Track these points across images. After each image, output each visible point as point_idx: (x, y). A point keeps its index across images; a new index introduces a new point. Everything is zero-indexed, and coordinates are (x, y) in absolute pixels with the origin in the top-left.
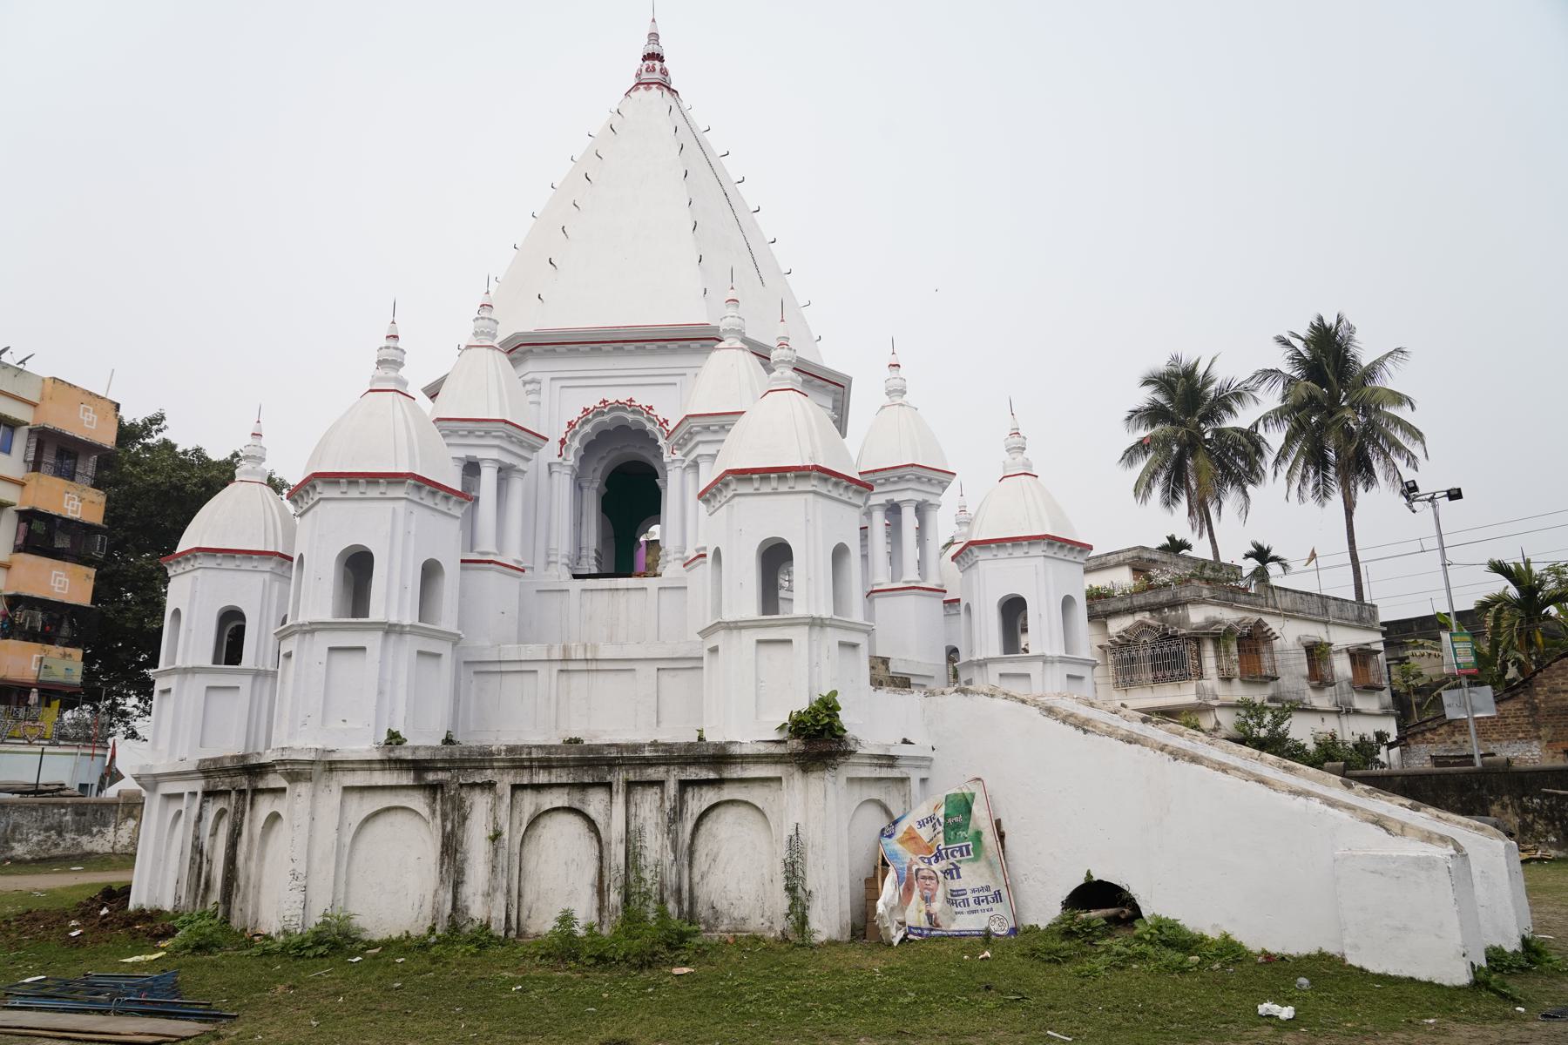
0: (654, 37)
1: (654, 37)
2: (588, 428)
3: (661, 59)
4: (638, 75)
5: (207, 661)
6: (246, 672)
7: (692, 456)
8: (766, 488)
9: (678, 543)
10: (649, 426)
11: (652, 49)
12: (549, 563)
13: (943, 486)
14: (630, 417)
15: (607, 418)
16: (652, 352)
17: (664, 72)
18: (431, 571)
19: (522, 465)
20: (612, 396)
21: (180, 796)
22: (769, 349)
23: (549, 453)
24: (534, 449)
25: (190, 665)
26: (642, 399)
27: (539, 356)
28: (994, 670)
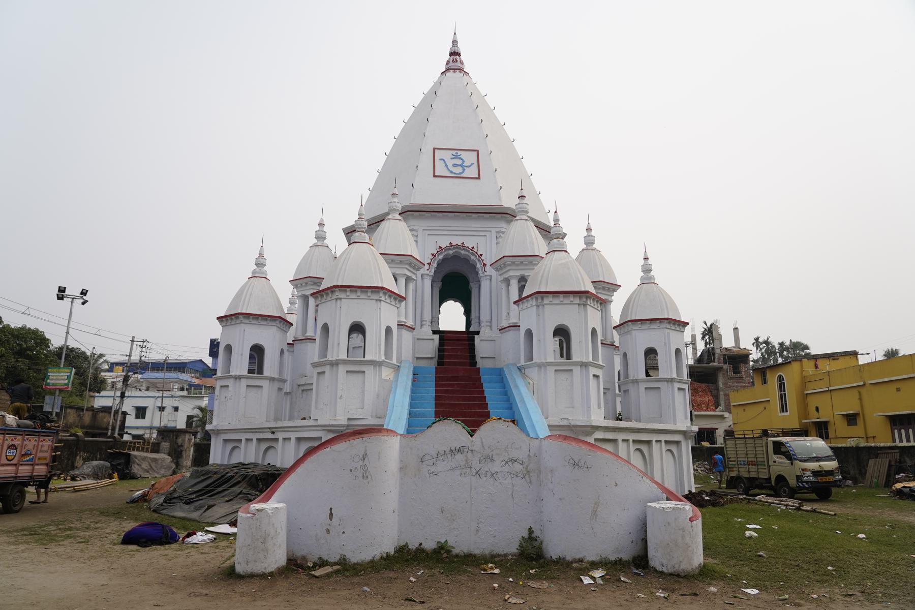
0: (455, 42)
1: (455, 42)
2: (441, 257)
3: (459, 55)
4: (448, 63)
5: (245, 373)
6: (266, 378)
7: (506, 276)
8: (566, 301)
9: (488, 318)
10: (473, 257)
11: (456, 50)
12: (422, 326)
13: (615, 291)
14: (463, 252)
15: (451, 252)
16: (463, 218)
17: (462, 63)
18: (389, 330)
19: (414, 277)
20: (457, 241)
21: (240, 441)
22: (550, 227)
23: (424, 270)
24: (419, 269)
25: (238, 374)
26: (469, 243)
27: (416, 218)
28: (642, 386)
